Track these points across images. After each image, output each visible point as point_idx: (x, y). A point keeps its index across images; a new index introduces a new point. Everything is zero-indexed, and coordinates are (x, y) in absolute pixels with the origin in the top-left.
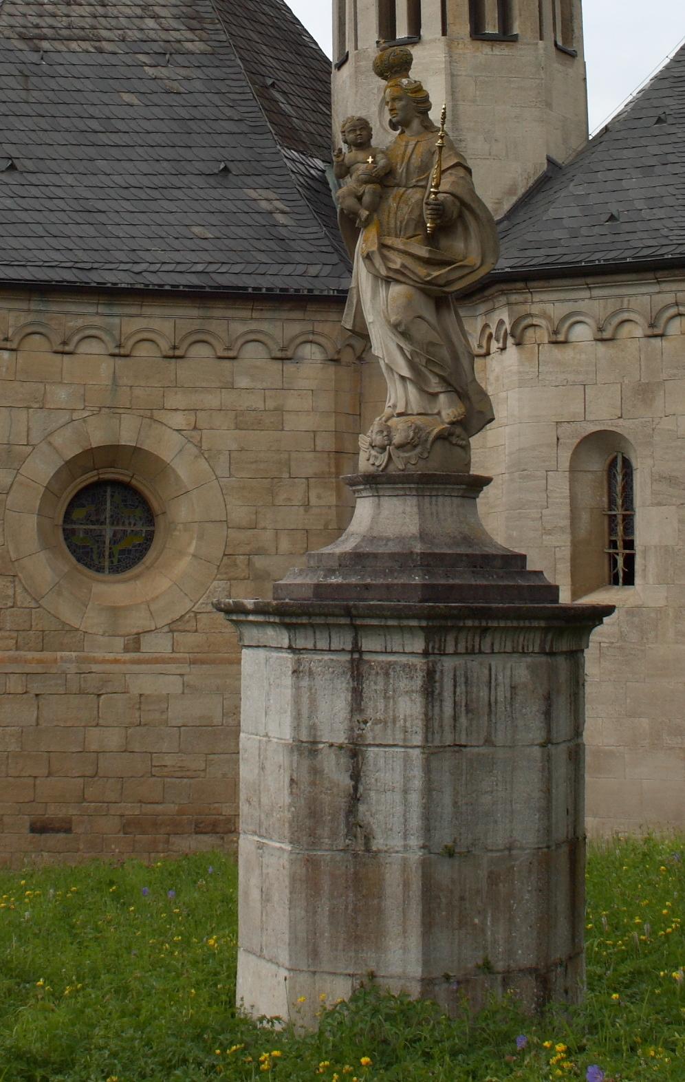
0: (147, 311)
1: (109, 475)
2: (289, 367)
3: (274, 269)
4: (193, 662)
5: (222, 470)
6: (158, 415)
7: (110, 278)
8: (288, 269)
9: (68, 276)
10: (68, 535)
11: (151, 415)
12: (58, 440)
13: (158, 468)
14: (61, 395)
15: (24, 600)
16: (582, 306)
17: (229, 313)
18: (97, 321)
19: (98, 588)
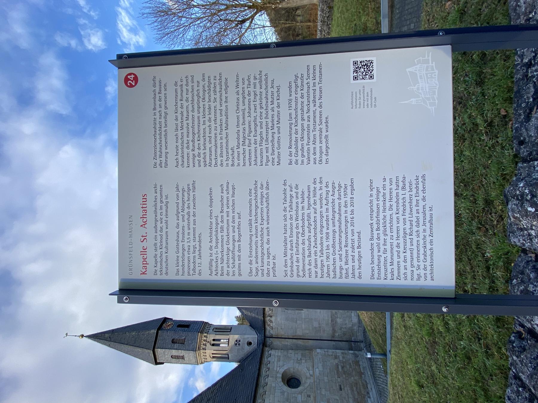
0: (262, 371)
3: (258, 355)
4: (314, 367)
6: (277, 371)
7: (257, 374)
12: (280, 386)
14: (273, 385)
15: (305, 391)
18: (263, 378)
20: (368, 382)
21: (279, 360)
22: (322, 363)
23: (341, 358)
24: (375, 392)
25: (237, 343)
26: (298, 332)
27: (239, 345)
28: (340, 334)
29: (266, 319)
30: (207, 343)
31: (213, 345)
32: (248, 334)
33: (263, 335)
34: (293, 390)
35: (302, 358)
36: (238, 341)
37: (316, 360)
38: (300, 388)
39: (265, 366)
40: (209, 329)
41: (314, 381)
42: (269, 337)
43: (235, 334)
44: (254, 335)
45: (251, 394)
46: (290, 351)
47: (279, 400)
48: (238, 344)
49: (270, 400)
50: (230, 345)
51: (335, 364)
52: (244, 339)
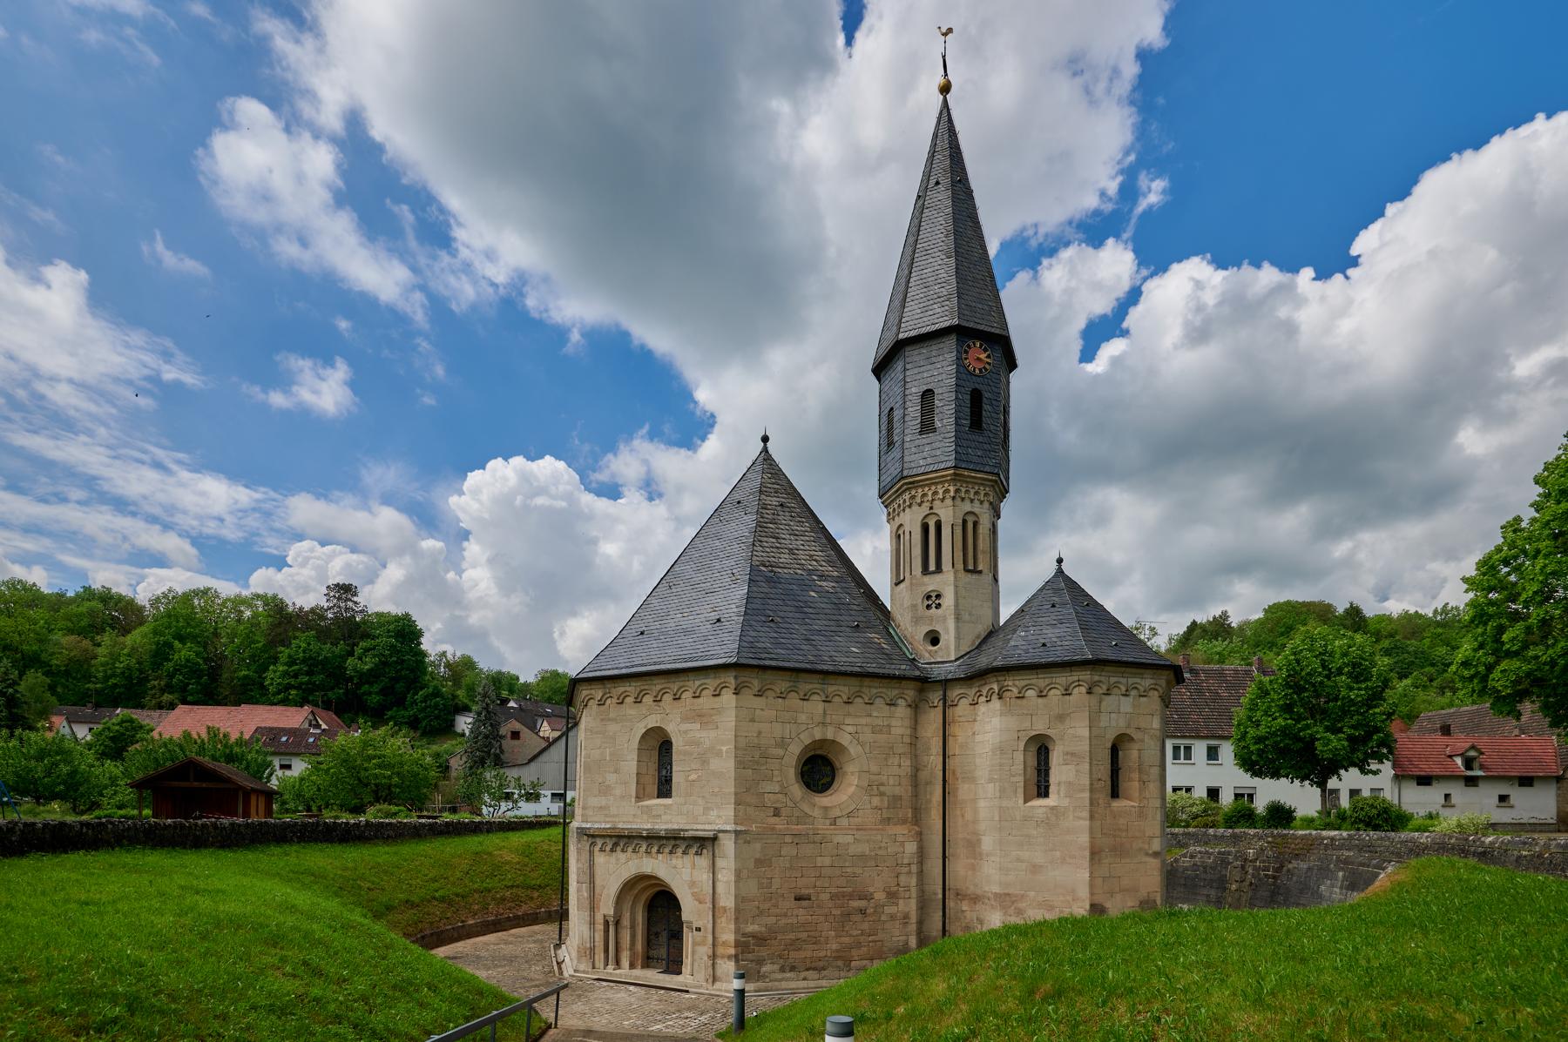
1: (818, 752)
2: (893, 708)
3: (888, 666)
4: (857, 829)
5: (867, 750)
7: (825, 667)
8: (893, 666)
9: (808, 666)
10: (802, 777)
11: (839, 727)
12: (802, 736)
13: (841, 749)
14: (803, 718)
16: (1034, 681)
17: (871, 684)
19: (817, 799)
20: (824, 973)
21: (875, 730)
22: (873, 854)
23: (889, 910)
24: (794, 986)
25: (934, 599)
26: (966, 786)
27: (929, 607)
28: (965, 917)
29: (992, 680)
30: (928, 504)
31: (925, 528)
32: (957, 628)
33: (950, 677)
34: (791, 773)
35: (886, 798)
36: (937, 602)
37: (879, 837)
38: (797, 790)
39: (854, 689)
40: (972, 501)
41: (818, 829)
42: (945, 695)
43: (956, 586)
44: (957, 648)
45: (771, 659)
46: (907, 763)
47: (763, 735)
48: (930, 602)
49: (762, 710)
50: (927, 579)
51: (871, 890)
52: (944, 619)
